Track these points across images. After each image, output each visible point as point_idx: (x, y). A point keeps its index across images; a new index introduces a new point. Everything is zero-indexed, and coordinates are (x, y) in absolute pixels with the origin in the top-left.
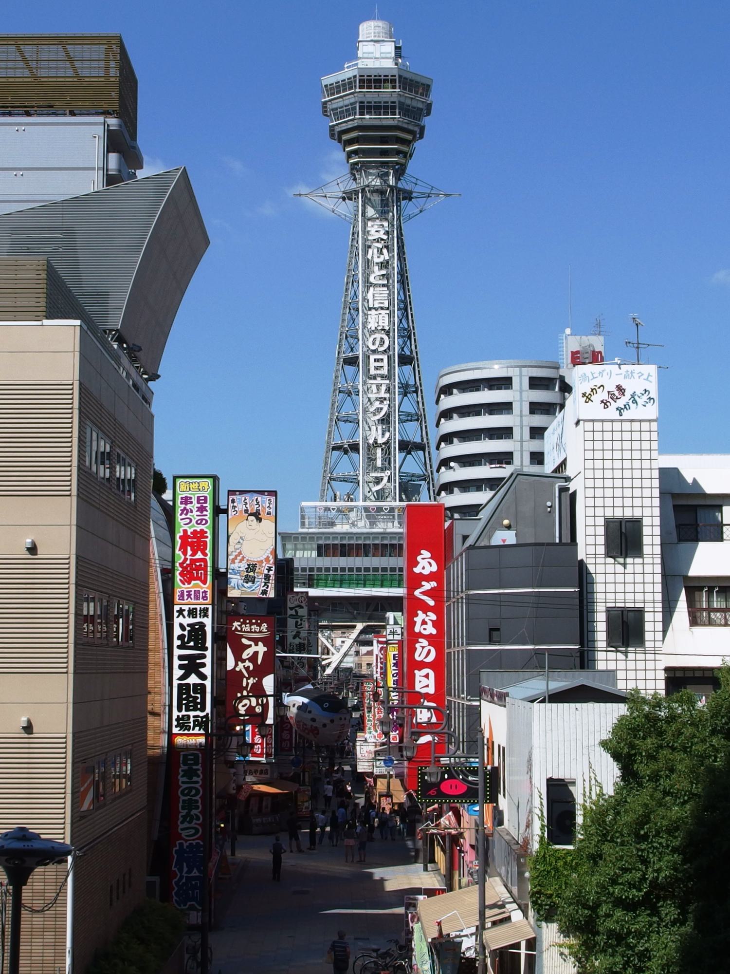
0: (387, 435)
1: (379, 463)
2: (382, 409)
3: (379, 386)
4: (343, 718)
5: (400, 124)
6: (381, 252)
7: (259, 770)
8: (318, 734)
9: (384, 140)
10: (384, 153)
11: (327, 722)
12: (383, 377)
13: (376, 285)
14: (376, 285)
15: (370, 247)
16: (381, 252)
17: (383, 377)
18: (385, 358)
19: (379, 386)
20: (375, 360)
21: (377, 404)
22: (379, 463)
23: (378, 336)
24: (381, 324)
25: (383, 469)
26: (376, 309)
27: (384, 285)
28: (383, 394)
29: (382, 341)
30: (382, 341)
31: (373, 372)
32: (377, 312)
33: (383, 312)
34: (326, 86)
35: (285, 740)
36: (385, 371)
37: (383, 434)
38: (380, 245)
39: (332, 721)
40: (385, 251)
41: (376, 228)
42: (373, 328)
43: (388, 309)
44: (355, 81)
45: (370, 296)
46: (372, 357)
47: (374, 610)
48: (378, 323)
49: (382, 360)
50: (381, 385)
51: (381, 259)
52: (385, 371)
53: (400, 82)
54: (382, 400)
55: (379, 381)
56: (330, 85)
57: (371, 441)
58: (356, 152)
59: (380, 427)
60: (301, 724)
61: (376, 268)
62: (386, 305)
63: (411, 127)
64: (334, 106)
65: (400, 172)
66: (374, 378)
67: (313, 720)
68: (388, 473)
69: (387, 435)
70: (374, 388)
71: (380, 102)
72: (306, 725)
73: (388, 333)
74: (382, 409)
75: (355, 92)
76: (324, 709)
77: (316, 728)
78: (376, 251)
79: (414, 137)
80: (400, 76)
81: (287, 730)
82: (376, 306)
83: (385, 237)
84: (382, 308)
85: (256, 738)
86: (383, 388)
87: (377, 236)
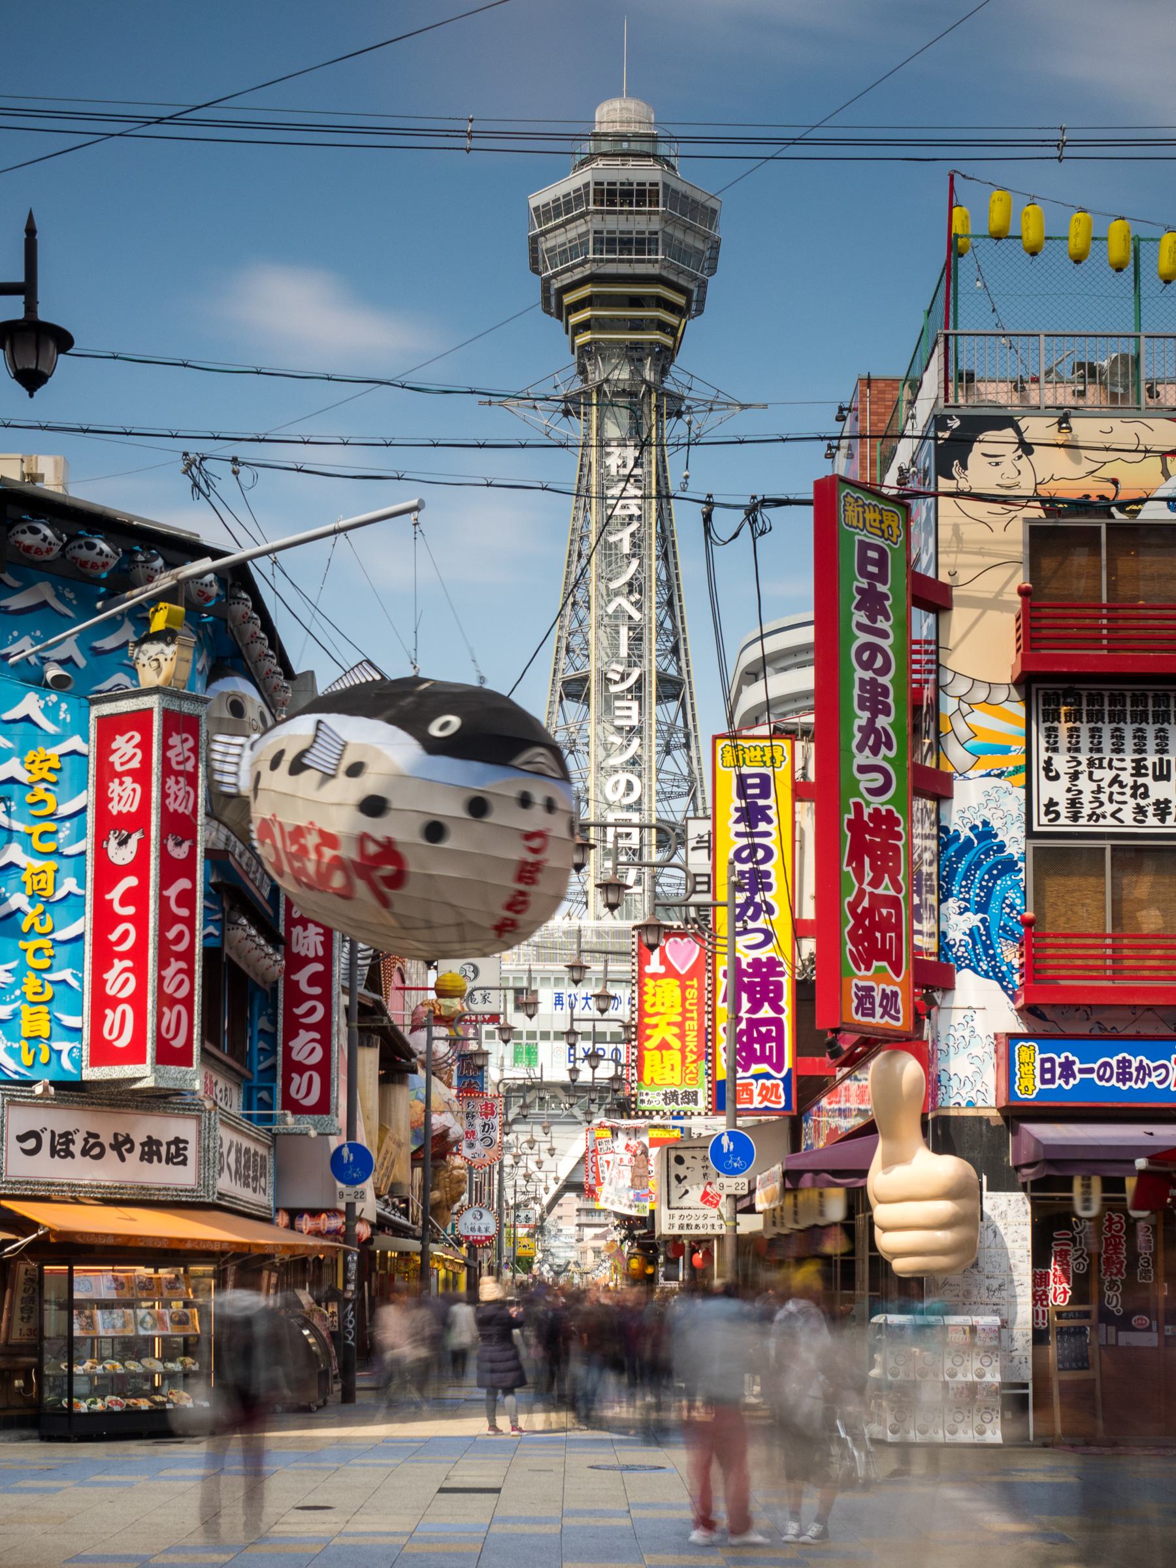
4: (538, 798)
5: (665, 273)
7: (139, 1138)
8: (397, 880)
9: (636, 302)
10: (637, 325)
11: (451, 808)
34: (536, 209)
35: (301, 1068)
39: (478, 807)
44: (587, 194)
53: (665, 195)
56: (544, 206)
58: (585, 326)
60: (312, 840)
63: (682, 281)
64: (550, 244)
65: (665, 357)
67: (373, 806)
71: (630, 232)
72: (329, 840)
75: (587, 213)
76: (433, 747)
77: (389, 852)
79: (689, 302)
80: (666, 186)
81: (309, 1028)
85: (110, 976)
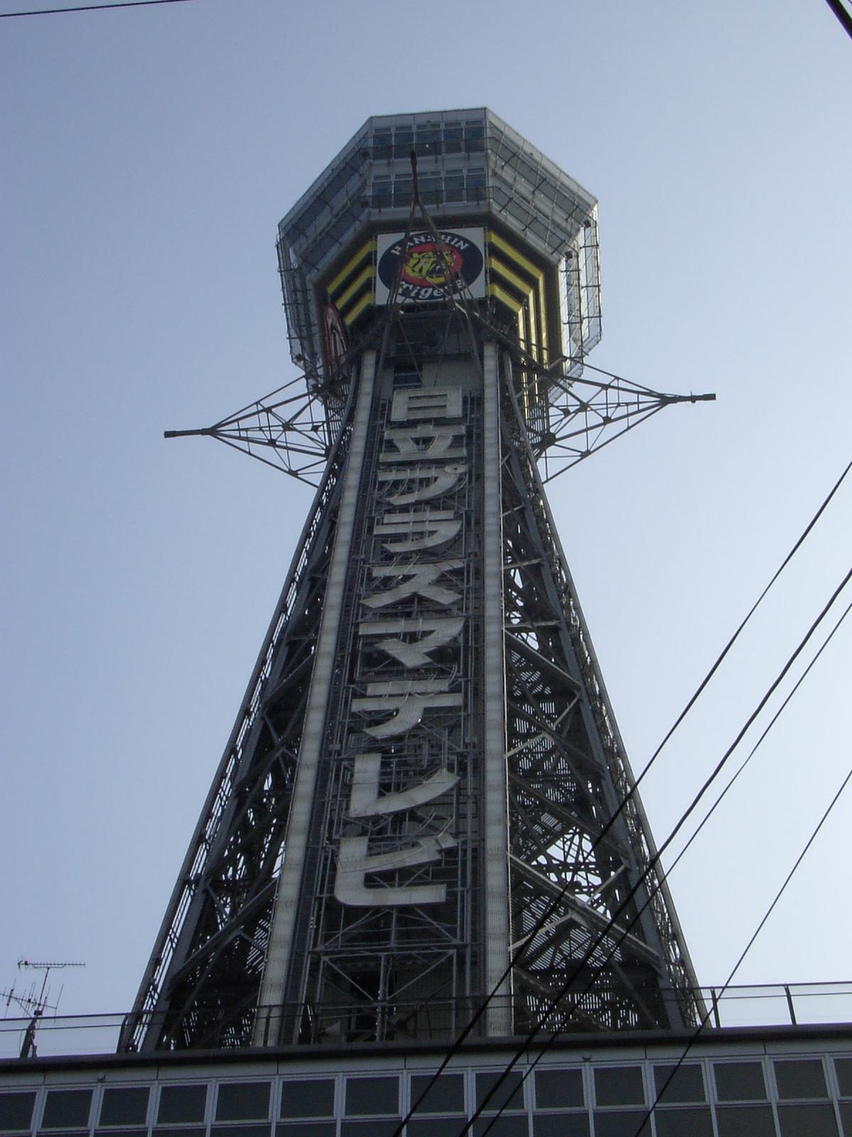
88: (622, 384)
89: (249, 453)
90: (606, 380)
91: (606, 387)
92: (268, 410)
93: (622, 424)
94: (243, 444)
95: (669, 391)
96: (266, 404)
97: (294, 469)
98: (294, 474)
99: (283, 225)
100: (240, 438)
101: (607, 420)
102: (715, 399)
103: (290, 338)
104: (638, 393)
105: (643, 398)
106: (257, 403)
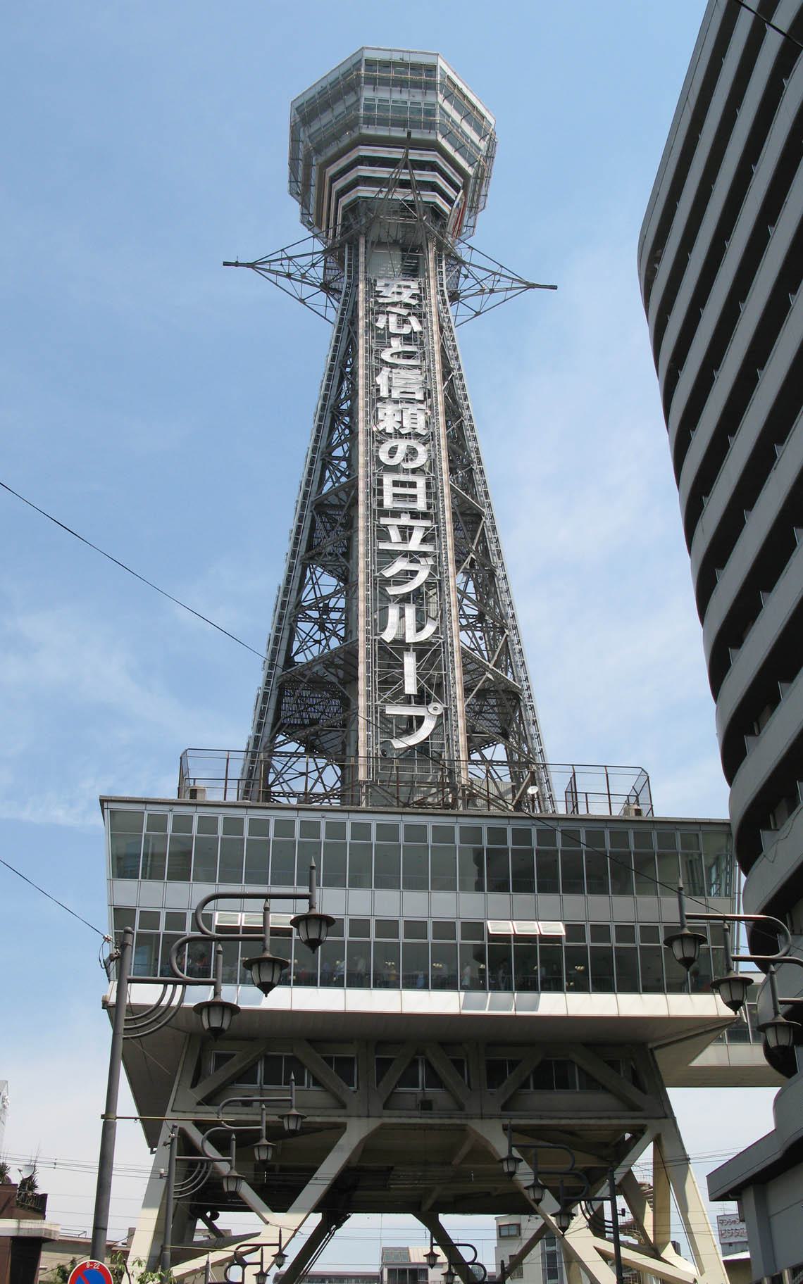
0: (430, 629)
1: (410, 688)
2: (414, 573)
3: (406, 532)
6: (404, 321)
12: (415, 515)
13: (393, 366)
14: (393, 366)
15: (378, 313)
16: (404, 321)
17: (415, 515)
18: (421, 482)
19: (406, 532)
20: (396, 484)
21: (401, 565)
22: (410, 688)
23: (402, 445)
24: (405, 423)
25: (422, 698)
26: (396, 402)
27: (415, 367)
28: (414, 544)
29: (412, 452)
30: (412, 452)
31: (388, 502)
32: (400, 406)
33: (412, 409)
36: (421, 505)
37: (420, 628)
38: (404, 312)
40: (413, 320)
41: (395, 289)
42: (389, 430)
43: (421, 402)
45: (381, 380)
46: (388, 479)
47: (401, 1083)
48: (401, 422)
49: (413, 485)
50: (411, 528)
51: (406, 330)
52: (421, 505)
54: (413, 556)
55: (405, 520)
57: (388, 636)
59: (410, 611)
61: (396, 344)
62: (419, 396)
66: (396, 514)
68: (436, 708)
69: (430, 629)
70: (395, 535)
73: (426, 440)
74: (414, 573)
78: (393, 319)
82: (395, 395)
83: (414, 302)
84: (411, 401)
86: (418, 535)
87: (396, 299)
88: (505, 272)
89: (276, 284)
90: (495, 268)
91: (495, 274)
92: (290, 258)
93: (501, 296)
94: (272, 277)
95: (531, 281)
96: (290, 253)
97: (303, 298)
98: (302, 301)
99: (296, 105)
100: (270, 271)
101: (492, 291)
102: (556, 289)
103: (290, 182)
104: (513, 279)
105: (516, 285)
106: (282, 250)
